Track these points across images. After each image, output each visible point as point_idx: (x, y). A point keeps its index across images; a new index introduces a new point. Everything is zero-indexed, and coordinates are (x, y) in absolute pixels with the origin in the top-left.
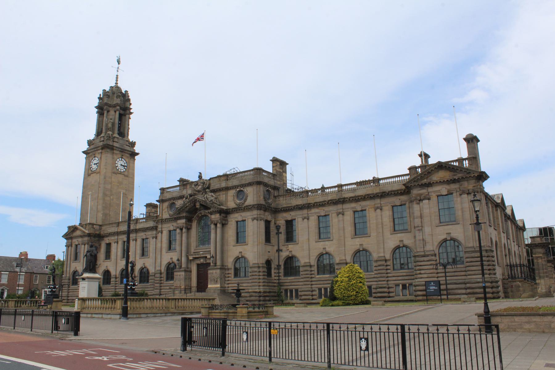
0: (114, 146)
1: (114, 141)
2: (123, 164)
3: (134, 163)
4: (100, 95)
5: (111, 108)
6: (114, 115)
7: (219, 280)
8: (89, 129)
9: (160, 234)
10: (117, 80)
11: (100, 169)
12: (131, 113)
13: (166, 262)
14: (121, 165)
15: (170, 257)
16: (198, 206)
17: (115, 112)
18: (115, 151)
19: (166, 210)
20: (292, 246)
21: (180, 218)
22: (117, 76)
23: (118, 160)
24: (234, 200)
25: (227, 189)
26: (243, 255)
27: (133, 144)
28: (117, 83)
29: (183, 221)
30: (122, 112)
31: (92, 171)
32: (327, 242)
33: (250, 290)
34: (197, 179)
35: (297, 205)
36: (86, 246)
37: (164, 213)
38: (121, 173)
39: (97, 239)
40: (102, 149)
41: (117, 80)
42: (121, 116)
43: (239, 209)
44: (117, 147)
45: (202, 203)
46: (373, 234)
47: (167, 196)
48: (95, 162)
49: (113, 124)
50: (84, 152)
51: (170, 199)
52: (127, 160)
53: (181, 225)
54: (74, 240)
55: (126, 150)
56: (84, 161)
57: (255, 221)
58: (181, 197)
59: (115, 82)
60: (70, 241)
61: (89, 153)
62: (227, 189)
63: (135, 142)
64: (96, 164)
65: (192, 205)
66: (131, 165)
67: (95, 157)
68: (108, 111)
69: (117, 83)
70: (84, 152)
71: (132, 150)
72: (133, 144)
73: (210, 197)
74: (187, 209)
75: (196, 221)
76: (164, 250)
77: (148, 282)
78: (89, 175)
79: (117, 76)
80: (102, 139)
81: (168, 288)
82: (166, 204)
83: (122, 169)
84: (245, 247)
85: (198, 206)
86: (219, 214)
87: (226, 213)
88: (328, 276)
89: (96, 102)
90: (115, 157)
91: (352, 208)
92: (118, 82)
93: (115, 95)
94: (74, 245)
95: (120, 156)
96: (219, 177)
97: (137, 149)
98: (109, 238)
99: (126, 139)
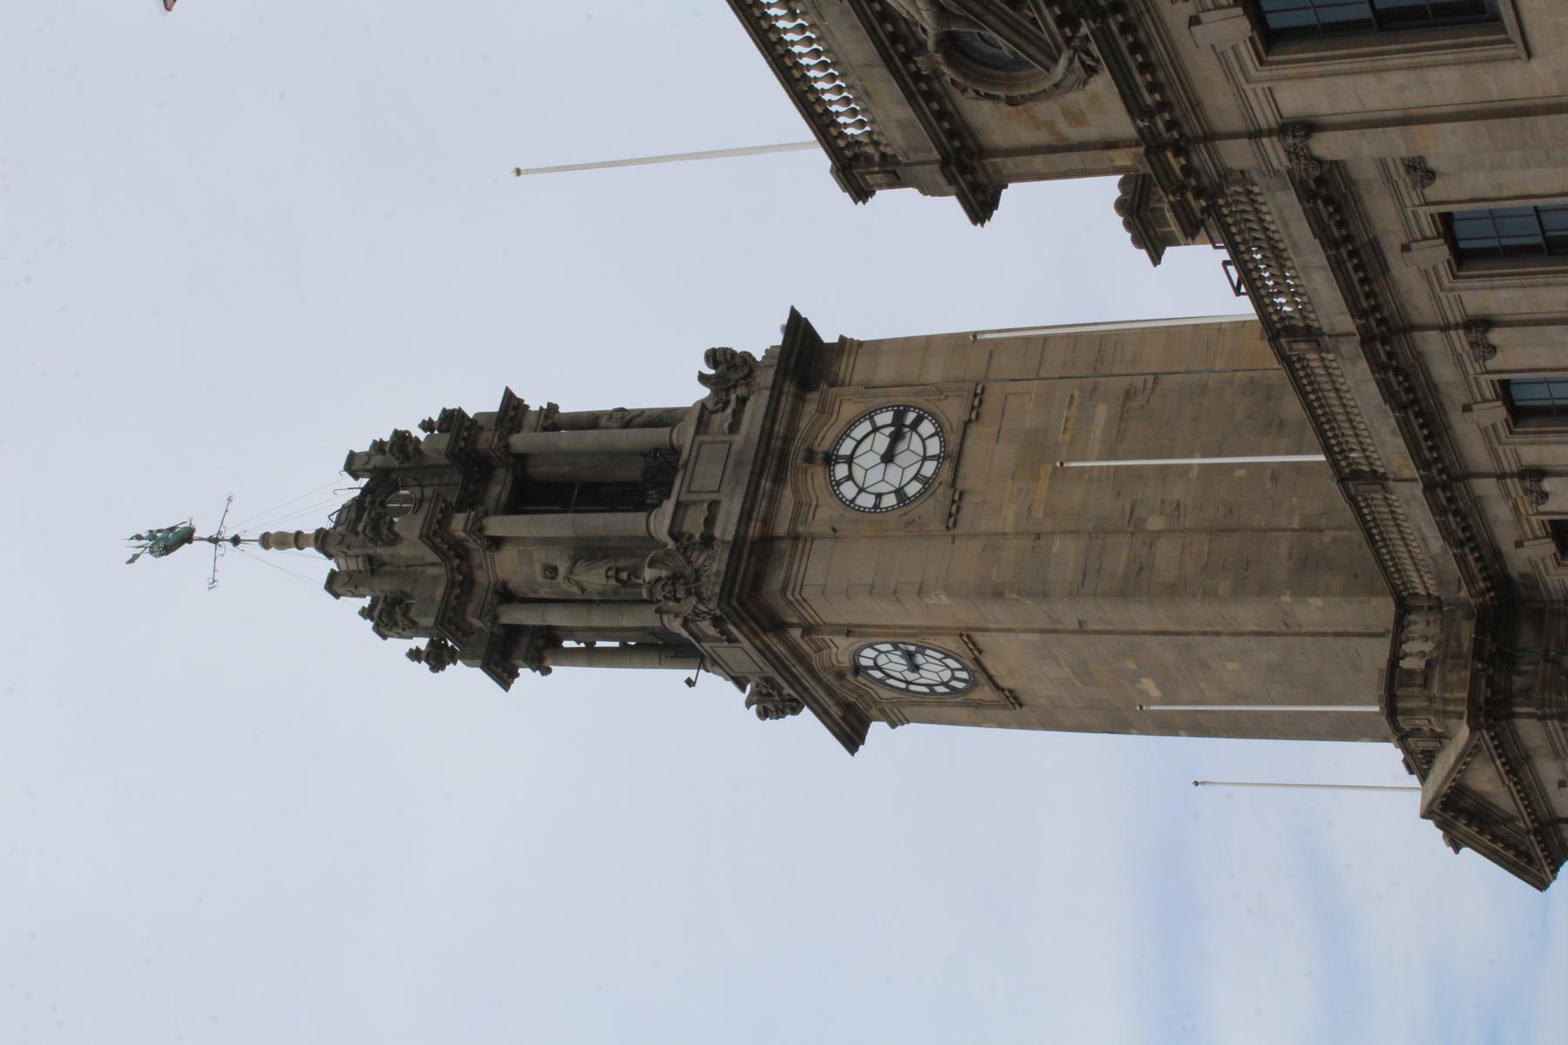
0: (739, 540)
1: (708, 541)
2: (882, 442)
3: (876, 346)
4: (415, 655)
5: (480, 576)
6: (525, 547)
8: (645, 731)
10: (298, 540)
11: (936, 631)
12: (512, 405)
14: (888, 458)
17: (496, 543)
18: (782, 527)
22: (266, 541)
23: (848, 490)
27: (727, 368)
30: (499, 488)
31: (972, 684)
37: (1092, 132)
38: (953, 458)
39: (1527, 636)
41: (298, 540)
42: (534, 492)
44: (746, 516)
47: (889, 117)
48: (895, 665)
49: (588, 551)
51: (920, 91)
52: (849, 410)
55: (767, 434)
56: (914, 732)
61: (849, 708)
63: (713, 357)
64: (909, 656)
66: (885, 372)
67: (858, 669)
68: (506, 595)
71: (766, 378)
72: (727, 368)
79: (266, 541)
80: (706, 626)
83: (924, 442)
89: (466, 678)
90: (826, 513)
92: (310, 529)
93: (382, 551)
95: (819, 471)
97: (759, 338)
98: (1505, 538)
99: (685, 436)
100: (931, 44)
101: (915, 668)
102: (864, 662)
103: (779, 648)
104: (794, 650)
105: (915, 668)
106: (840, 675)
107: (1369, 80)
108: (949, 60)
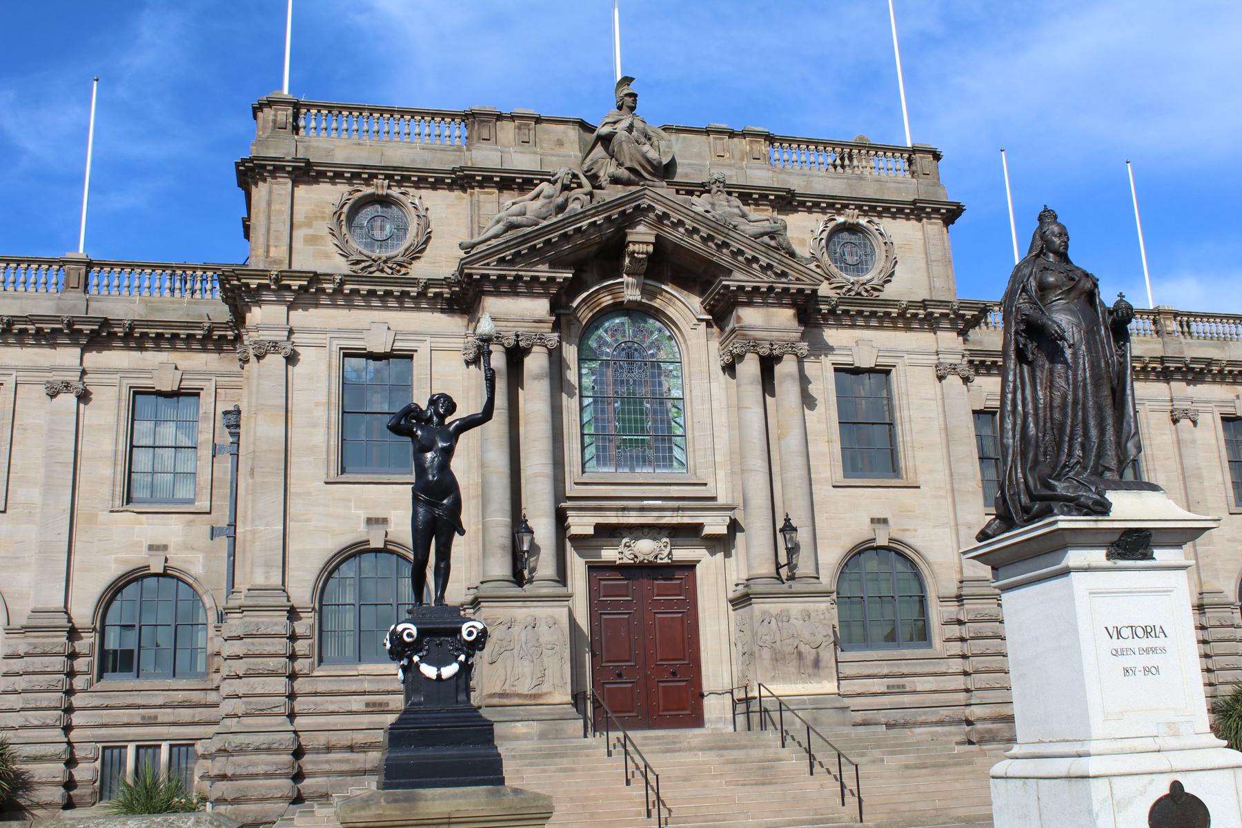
7: (827, 655)
15: (363, 515)
16: (641, 238)
19: (322, 227)
21: (512, 288)
25: (787, 201)
29: (540, 307)
33: (977, 711)
45: (677, 236)
58: (463, 180)
62: (787, 201)
81: (357, 703)
85: (641, 238)
86: (790, 312)
91: (1222, 403)
100: (389, 191)
107: (323, 398)
108: (373, 194)
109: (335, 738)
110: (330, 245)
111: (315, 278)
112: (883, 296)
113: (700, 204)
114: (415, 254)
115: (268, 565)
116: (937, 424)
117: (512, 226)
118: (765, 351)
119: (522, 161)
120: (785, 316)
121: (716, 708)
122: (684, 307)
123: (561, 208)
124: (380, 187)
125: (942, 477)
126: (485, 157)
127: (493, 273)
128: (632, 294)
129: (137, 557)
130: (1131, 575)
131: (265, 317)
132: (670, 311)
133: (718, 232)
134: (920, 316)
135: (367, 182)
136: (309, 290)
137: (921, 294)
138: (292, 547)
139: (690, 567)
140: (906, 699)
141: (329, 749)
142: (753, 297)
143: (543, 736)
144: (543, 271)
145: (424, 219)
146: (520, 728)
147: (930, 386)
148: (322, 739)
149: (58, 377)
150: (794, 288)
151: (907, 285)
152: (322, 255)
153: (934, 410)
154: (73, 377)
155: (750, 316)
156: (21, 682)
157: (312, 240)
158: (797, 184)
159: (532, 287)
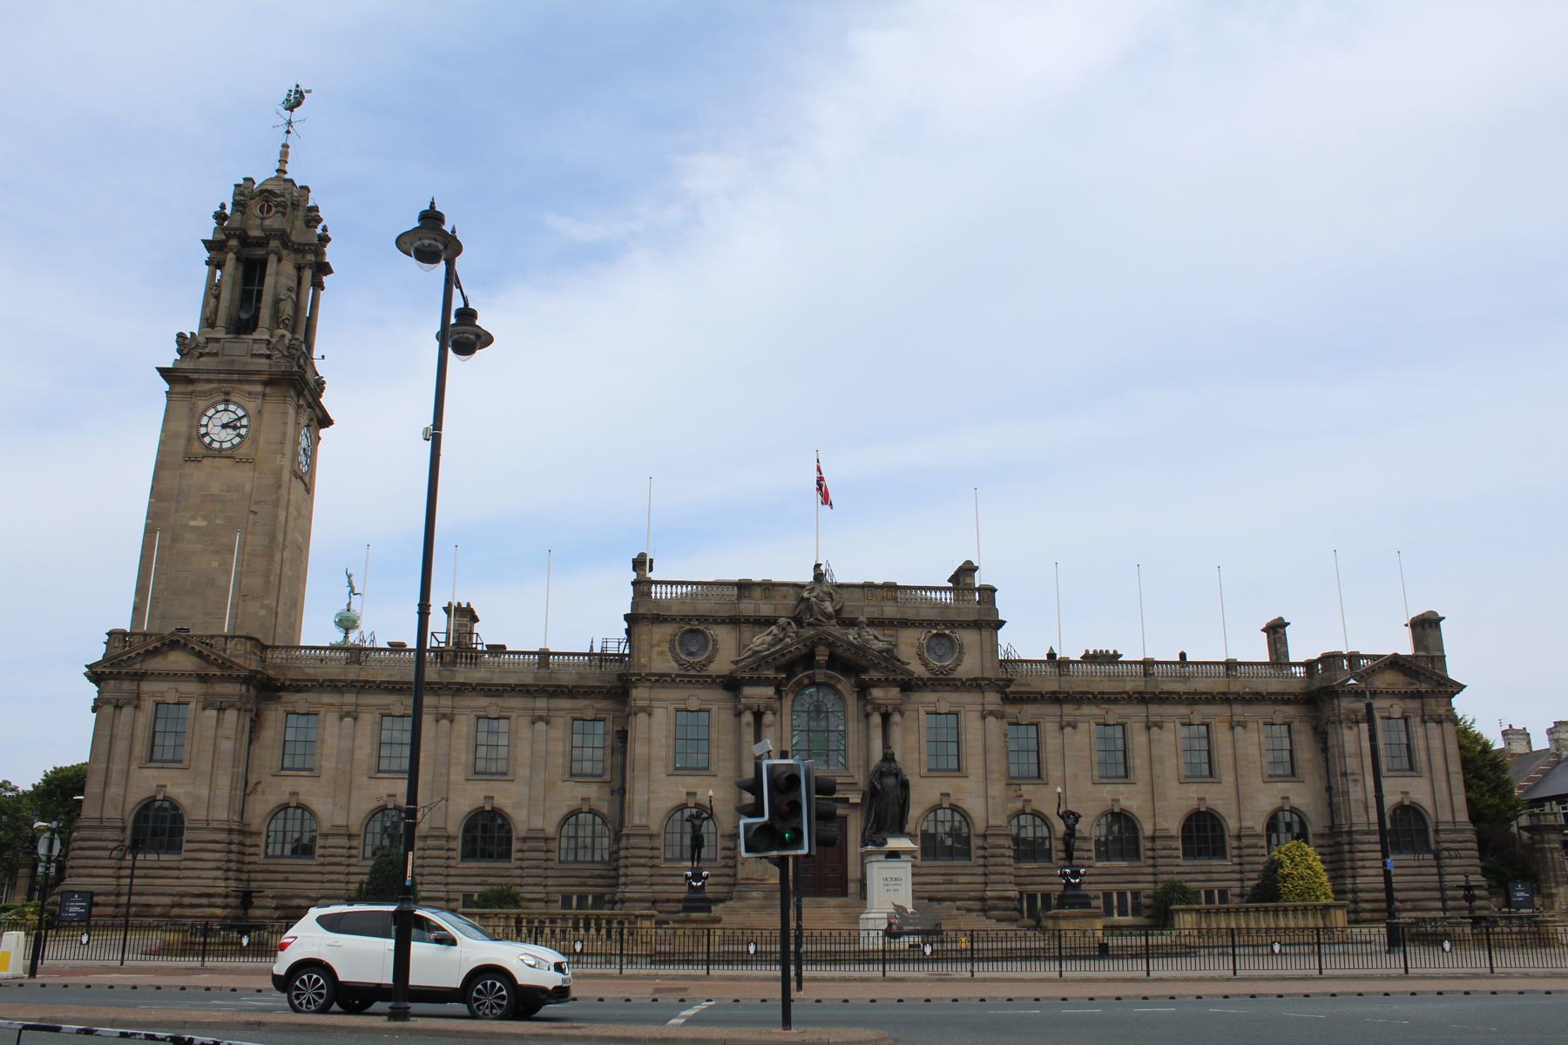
9: (642, 717)
10: (283, 161)
13: (670, 805)
15: (684, 790)
16: (822, 655)
19: (666, 647)
20: (1030, 788)
22: (285, 146)
24: (921, 657)
25: (905, 623)
26: (953, 800)
28: (281, 171)
29: (770, 691)
32: (1121, 788)
34: (807, 577)
35: (1054, 692)
36: (231, 715)
37: (655, 656)
40: (266, 384)
41: (283, 161)
43: (943, 682)
45: (839, 651)
46: (1228, 779)
50: (163, 372)
53: (762, 702)
54: (146, 687)
57: (991, 720)
58: (735, 621)
59: (277, 166)
60: (127, 686)
62: (905, 623)
65: (804, 650)
67: (227, 402)
68: (279, 260)
69: (281, 171)
70: (163, 372)
73: (876, 640)
74: (783, 660)
75: (791, 697)
76: (659, 771)
77: (506, 855)
78: (191, 459)
79: (285, 146)
82: (663, 632)
84: (961, 782)
87: (908, 686)
88: (1124, 864)
91: (1182, 717)
92: (287, 168)
93: (301, 213)
94: (148, 705)
96: (868, 587)
101: (225, 426)
102: (232, 407)
103: (256, 377)
104: (249, 382)
105: (225, 426)
106: (227, 393)
109: (671, 896)
110: (669, 656)
111: (662, 675)
112: (955, 675)
113: (852, 635)
114: (710, 660)
115: (640, 815)
116: (980, 744)
117: (756, 652)
118: (883, 710)
119: (766, 610)
120: (894, 692)
121: (853, 887)
122: (845, 685)
123: (781, 640)
124: (695, 625)
125: (981, 771)
126: (747, 607)
127: (747, 676)
128: (820, 678)
129: (576, 804)
130: (893, 863)
131: (639, 694)
132: (839, 686)
133: (862, 649)
134: (974, 685)
135: (688, 623)
136: (662, 679)
137: (978, 674)
138: (652, 806)
139: (845, 818)
140: (953, 887)
141: (668, 901)
142: (877, 684)
143: (765, 898)
144: (771, 673)
145: (715, 642)
146: (754, 894)
147: (978, 724)
148: (665, 896)
149: (537, 713)
150: (899, 677)
151: (969, 666)
152: (663, 663)
153: (979, 735)
154: (544, 713)
155: (877, 693)
156: (526, 863)
157: (661, 653)
158: (910, 614)
159: (766, 682)
